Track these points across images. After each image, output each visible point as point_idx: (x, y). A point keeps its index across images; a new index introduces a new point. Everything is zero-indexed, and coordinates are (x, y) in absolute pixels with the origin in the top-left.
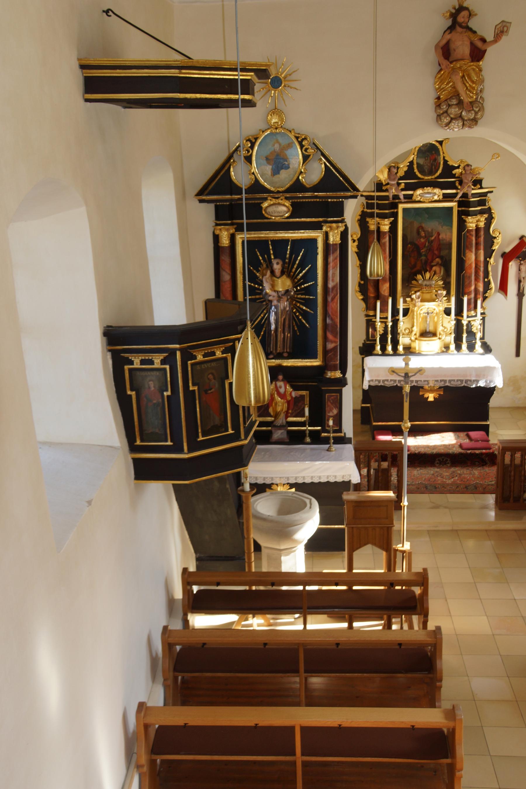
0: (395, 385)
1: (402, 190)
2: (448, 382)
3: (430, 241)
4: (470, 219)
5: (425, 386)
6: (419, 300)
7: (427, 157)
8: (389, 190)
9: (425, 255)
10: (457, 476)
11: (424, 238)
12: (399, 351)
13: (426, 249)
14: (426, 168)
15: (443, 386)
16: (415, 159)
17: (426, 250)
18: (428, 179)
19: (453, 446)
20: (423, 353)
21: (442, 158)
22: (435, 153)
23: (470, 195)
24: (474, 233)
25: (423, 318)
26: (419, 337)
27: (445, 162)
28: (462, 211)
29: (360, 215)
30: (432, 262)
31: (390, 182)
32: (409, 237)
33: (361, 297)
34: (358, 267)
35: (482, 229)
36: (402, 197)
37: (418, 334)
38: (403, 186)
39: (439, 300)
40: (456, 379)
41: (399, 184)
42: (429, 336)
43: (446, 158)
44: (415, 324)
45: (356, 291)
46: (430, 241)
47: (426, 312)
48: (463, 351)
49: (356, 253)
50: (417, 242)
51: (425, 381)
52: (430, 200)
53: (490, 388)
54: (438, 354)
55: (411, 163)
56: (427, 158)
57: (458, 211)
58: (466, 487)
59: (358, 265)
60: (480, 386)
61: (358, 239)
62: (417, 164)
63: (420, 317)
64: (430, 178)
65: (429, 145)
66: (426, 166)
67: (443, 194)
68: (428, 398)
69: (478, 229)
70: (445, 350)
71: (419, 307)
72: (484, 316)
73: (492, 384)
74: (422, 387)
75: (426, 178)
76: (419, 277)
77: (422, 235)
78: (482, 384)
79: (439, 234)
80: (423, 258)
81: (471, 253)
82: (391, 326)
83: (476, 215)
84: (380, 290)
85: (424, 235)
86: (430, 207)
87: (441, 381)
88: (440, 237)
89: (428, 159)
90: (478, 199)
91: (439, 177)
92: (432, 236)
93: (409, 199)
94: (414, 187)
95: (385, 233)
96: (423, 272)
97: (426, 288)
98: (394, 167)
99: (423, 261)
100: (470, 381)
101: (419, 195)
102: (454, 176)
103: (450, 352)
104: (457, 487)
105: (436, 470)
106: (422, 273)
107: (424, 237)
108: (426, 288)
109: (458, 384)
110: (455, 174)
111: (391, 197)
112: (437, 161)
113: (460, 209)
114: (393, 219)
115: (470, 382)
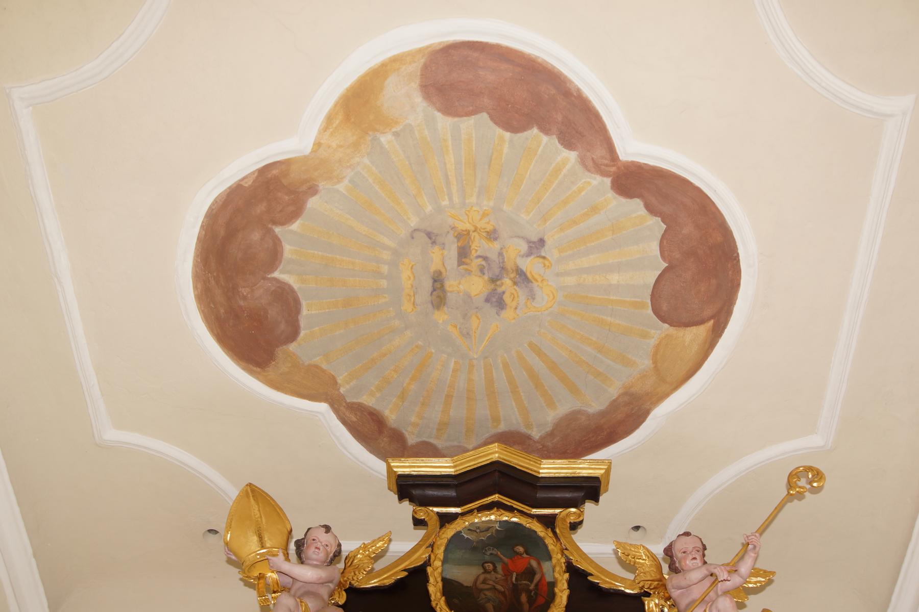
21: (558, 559)
22: (526, 552)
65: (497, 526)
66: (489, 594)
89: (495, 567)
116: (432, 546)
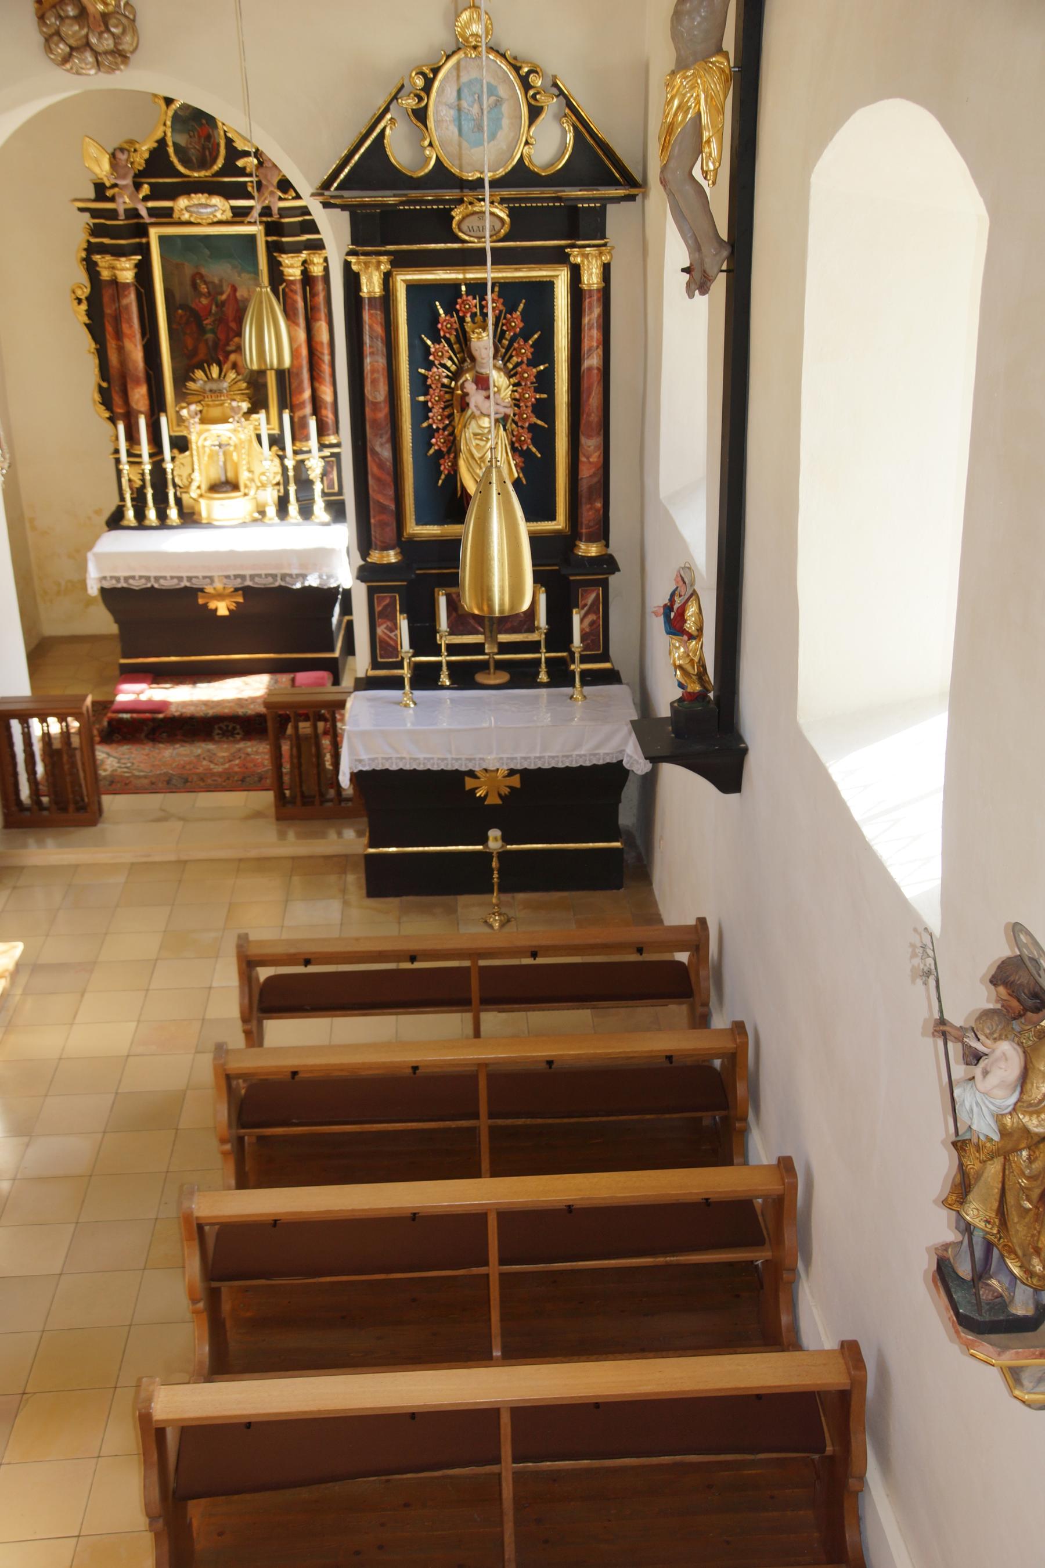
0: (149, 585)
1: (146, 199)
2: (248, 578)
3: (219, 302)
4: (286, 259)
5: (206, 587)
6: (197, 420)
7: (192, 131)
8: (117, 198)
9: (213, 331)
10: (240, 758)
11: (206, 297)
12: (171, 519)
13: (213, 319)
14: (193, 155)
15: (240, 586)
16: (169, 134)
17: (214, 321)
18: (200, 177)
19: (253, 700)
20: (216, 523)
21: (222, 133)
23: (275, 211)
24: (298, 287)
25: (211, 457)
26: (206, 492)
27: (229, 141)
28: (274, 242)
29: (85, 249)
30: (228, 344)
31: (119, 182)
32: (177, 296)
33: (107, 415)
34: (93, 353)
35: (320, 279)
36: (143, 212)
37: (204, 487)
38: (146, 189)
39: (234, 420)
40: (263, 572)
41: (137, 186)
42: (225, 489)
43: (229, 135)
44: (196, 467)
45: (94, 401)
46: (219, 302)
47: (217, 443)
48: (291, 518)
49: (86, 325)
50: (193, 306)
51: (205, 577)
52: (210, 221)
53: (330, 589)
54: (244, 524)
55: (162, 142)
56: (191, 133)
57: (267, 242)
58: (243, 780)
59: (93, 350)
60: (310, 587)
61: (87, 299)
62: (175, 144)
63: (204, 452)
64: (203, 173)
67: (232, 208)
68: (216, 610)
69: (307, 278)
70: (260, 517)
71: (200, 434)
72: (336, 450)
73: (332, 581)
74: (202, 590)
75: (196, 174)
76: (199, 374)
77: (202, 290)
78: (313, 581)
79: (234, 289)
80: (210, 336)
81: (296, 328)
82: (150, 471)
83: (300, 251)
84: (130, 400)
85: (206, 290)
86: (212, 233)
87: (236, 576)
88: (238, 294)
90: (300, 219)
91: (217, 174)
92: (222, 293)
93: (165, 216)
94: (173, 193)
95: (126, 286)
96: (206, 365)
97: (211, 397)
98: (122, 150)
99: (210, 343)
100: (291, 576)
101: (187, 208)
102: (242, 172)
103: (266, 520)
104: (228, 778)
105: (211, 746)
106: (204, 367)
107: (207, 295)
108: (211, 397)
109: (269, 583)
110: (244, 168)
111: (121, 212)
112: (212, 140)
113: (270, 239)
114: (139, 257)
115: (259, 579)
116: (165, 124)
